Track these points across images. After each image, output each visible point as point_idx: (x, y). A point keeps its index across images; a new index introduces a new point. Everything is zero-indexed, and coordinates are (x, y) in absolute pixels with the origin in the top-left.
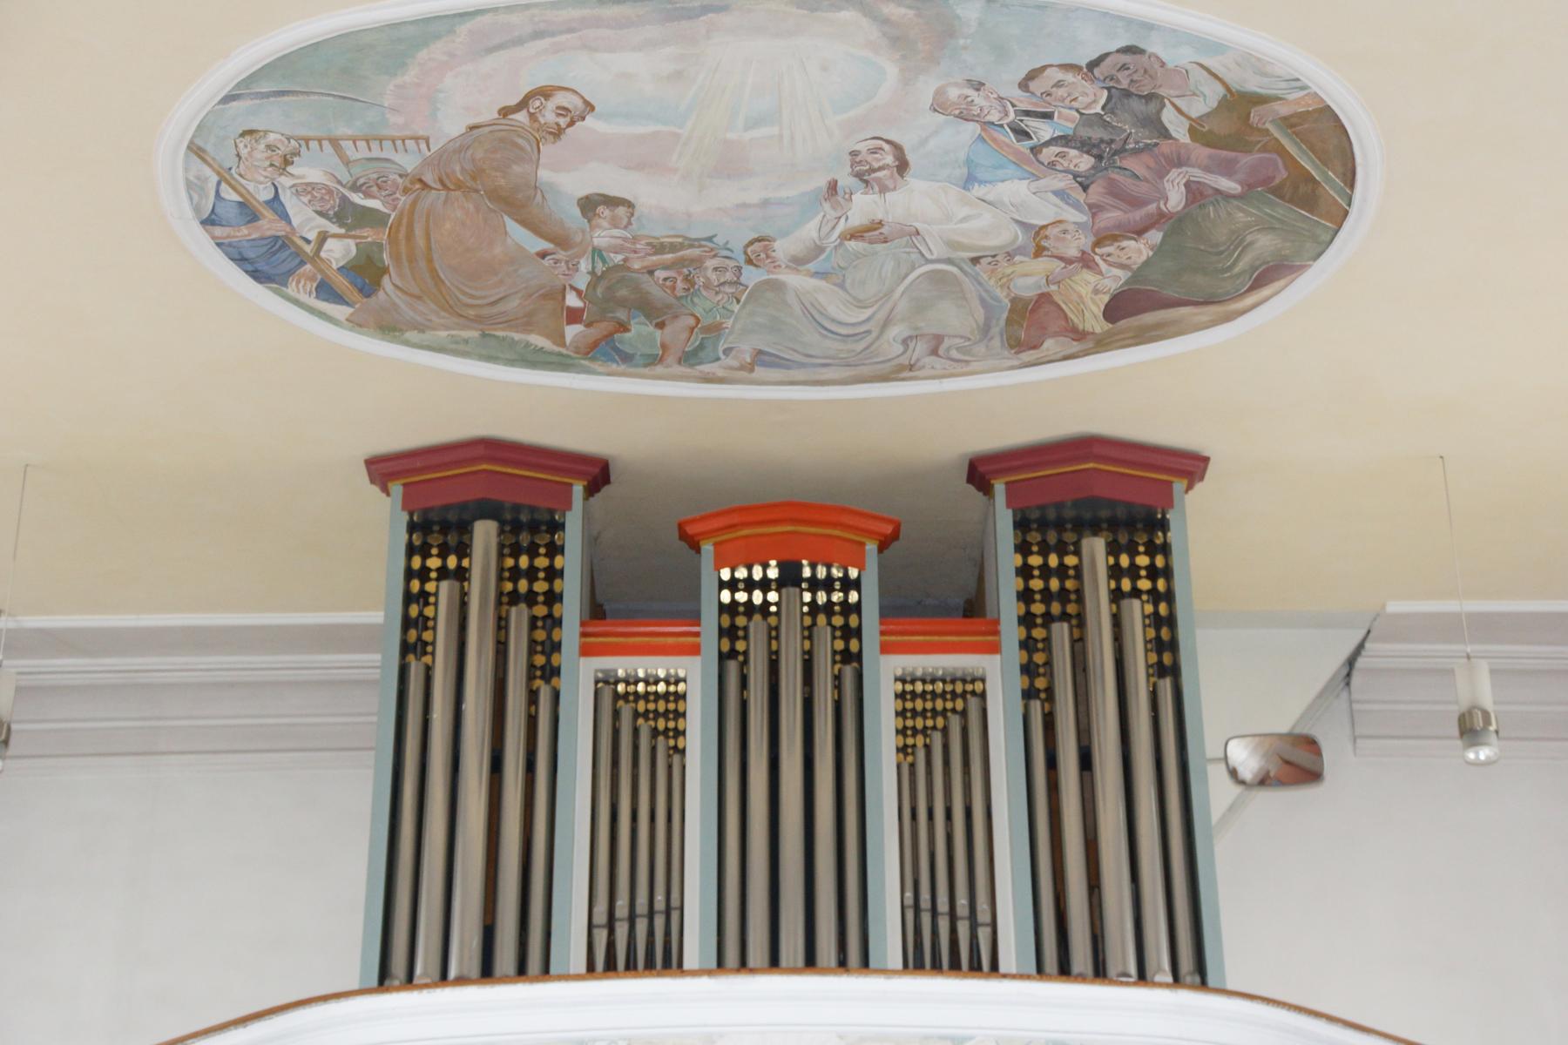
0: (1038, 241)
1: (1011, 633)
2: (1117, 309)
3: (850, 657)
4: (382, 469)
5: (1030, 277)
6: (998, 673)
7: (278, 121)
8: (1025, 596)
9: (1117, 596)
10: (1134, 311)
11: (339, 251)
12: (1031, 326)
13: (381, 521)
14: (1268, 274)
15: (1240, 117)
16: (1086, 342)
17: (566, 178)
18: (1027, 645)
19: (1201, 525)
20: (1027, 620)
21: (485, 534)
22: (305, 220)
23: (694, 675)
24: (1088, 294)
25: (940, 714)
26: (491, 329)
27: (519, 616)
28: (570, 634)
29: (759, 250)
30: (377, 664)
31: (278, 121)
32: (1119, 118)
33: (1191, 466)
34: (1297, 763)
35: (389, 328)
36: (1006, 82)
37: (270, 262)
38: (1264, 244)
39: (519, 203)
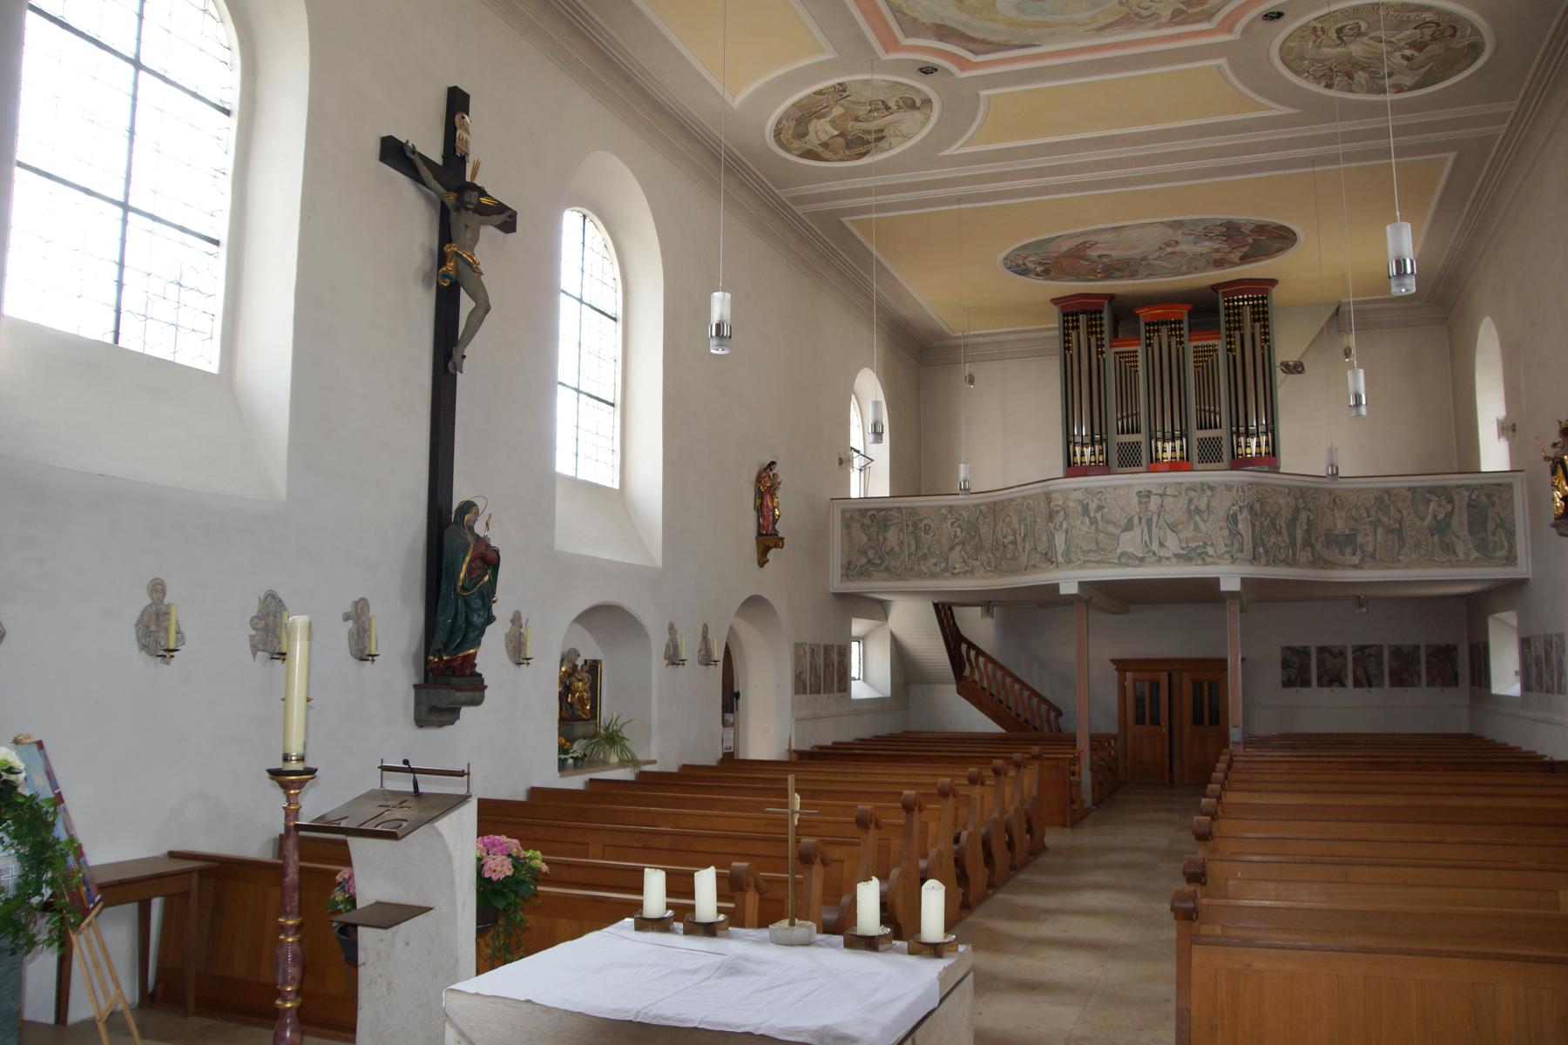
0: (1217, 251)
1: (1223, 332)
2: (1242, 258)
3: (1181, 343)
4: (1055, 301)
5: (1218, 256)
6: (1220, 344)
7: (1023, 253)
8: (1228, 322)
9: (1254, 320)
10: (1245, 259)
11: (1039, 269)
12: (1219, 263)
13: (1055, 311)
14: (1280, 250)
15: (1261, 229)
16: (1235, 264)
17: (1093, 254)
18: (1229, 336)
19: (1277, 295)
20: (1228, 329)
21: (1082, 318)
22: (1031, 266)
23: (1140, 350)
24: (1235, 256)
25: (1204, 355)
26: (1079, 277)
27: (1093, 340)
28: (1106, 342)
29: (1145, 258)
30: (1056, 345)
31: (1023, 253)
32: (1231, 231)
33: (1273, 282)
34: (1296, 368)
35: (1053, 279)
36: (1200, 229)
37: (1024, 272)
38: (1277, 246)
39: (1084, 258)
